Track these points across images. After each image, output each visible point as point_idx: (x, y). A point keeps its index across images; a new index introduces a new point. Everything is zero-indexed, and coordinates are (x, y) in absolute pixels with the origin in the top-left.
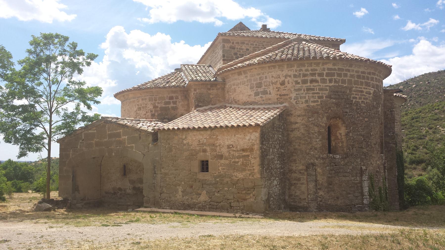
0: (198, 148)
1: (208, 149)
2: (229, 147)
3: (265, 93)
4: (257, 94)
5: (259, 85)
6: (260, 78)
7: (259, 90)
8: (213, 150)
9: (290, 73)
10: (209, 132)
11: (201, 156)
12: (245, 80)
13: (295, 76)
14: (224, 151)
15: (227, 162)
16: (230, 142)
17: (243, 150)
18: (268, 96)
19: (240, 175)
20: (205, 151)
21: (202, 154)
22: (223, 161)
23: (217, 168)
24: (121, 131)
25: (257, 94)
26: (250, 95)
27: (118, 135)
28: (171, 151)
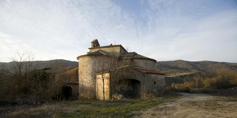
0: (154, 78)
1: (156, 79)
2: (160, 78)
3: (147, 66)
4: (145, 66)
5: (146, 64)
6: (146, 62)
7: (146, 65)
8: (157, 79)
9: (152, 62)
10: (156, 75)
11: (155, 80)
12: (142, 61)
13: (152, 63)
14: (159, 79)
15: (159, 82)
16: (160, 77)
17: (162, 79)
18: (148, 67)
19: (161, 85)
20: (155, 79)
21: (155, 80)
22: (159, 82)
23: (158, 83)
24: (135, 71)
25: (145, 66)
26: (144, 66)
27: (134, 72)
28: (148, 79)
